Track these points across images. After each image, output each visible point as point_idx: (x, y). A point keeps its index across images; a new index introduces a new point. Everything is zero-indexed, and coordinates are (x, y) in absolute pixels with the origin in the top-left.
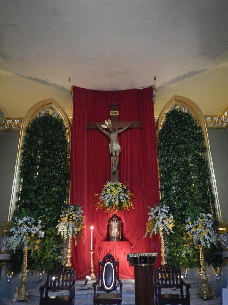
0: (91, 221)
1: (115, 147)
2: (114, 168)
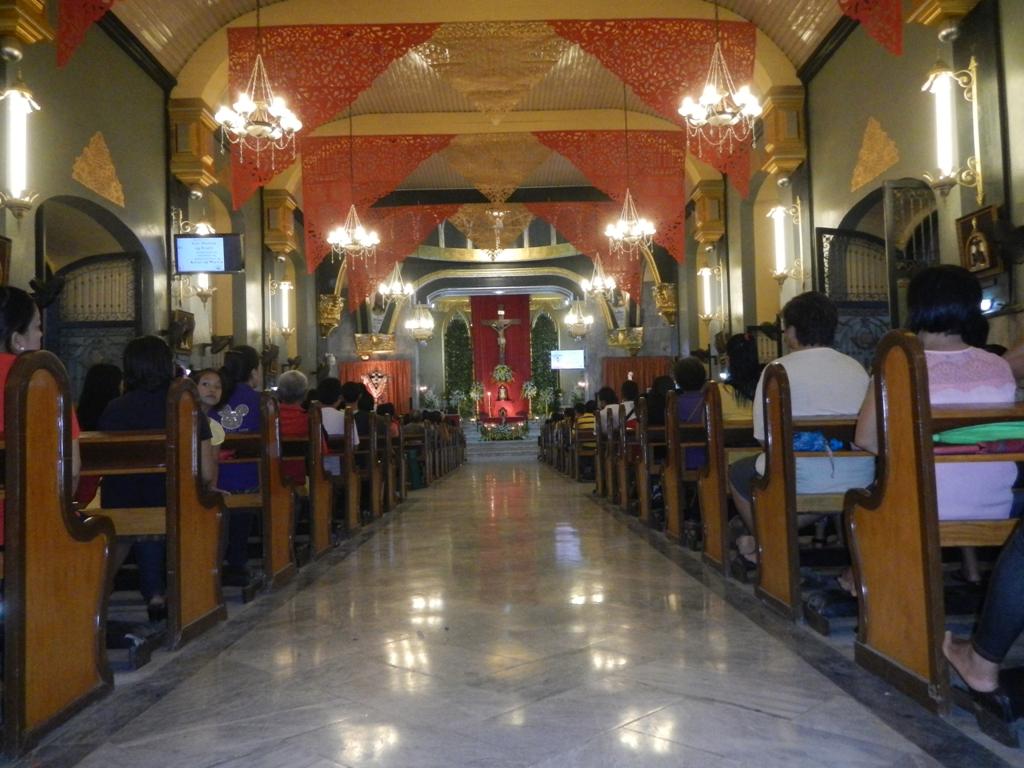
0: (488, 390)
1: (502, 341)
2: (502, 356)
